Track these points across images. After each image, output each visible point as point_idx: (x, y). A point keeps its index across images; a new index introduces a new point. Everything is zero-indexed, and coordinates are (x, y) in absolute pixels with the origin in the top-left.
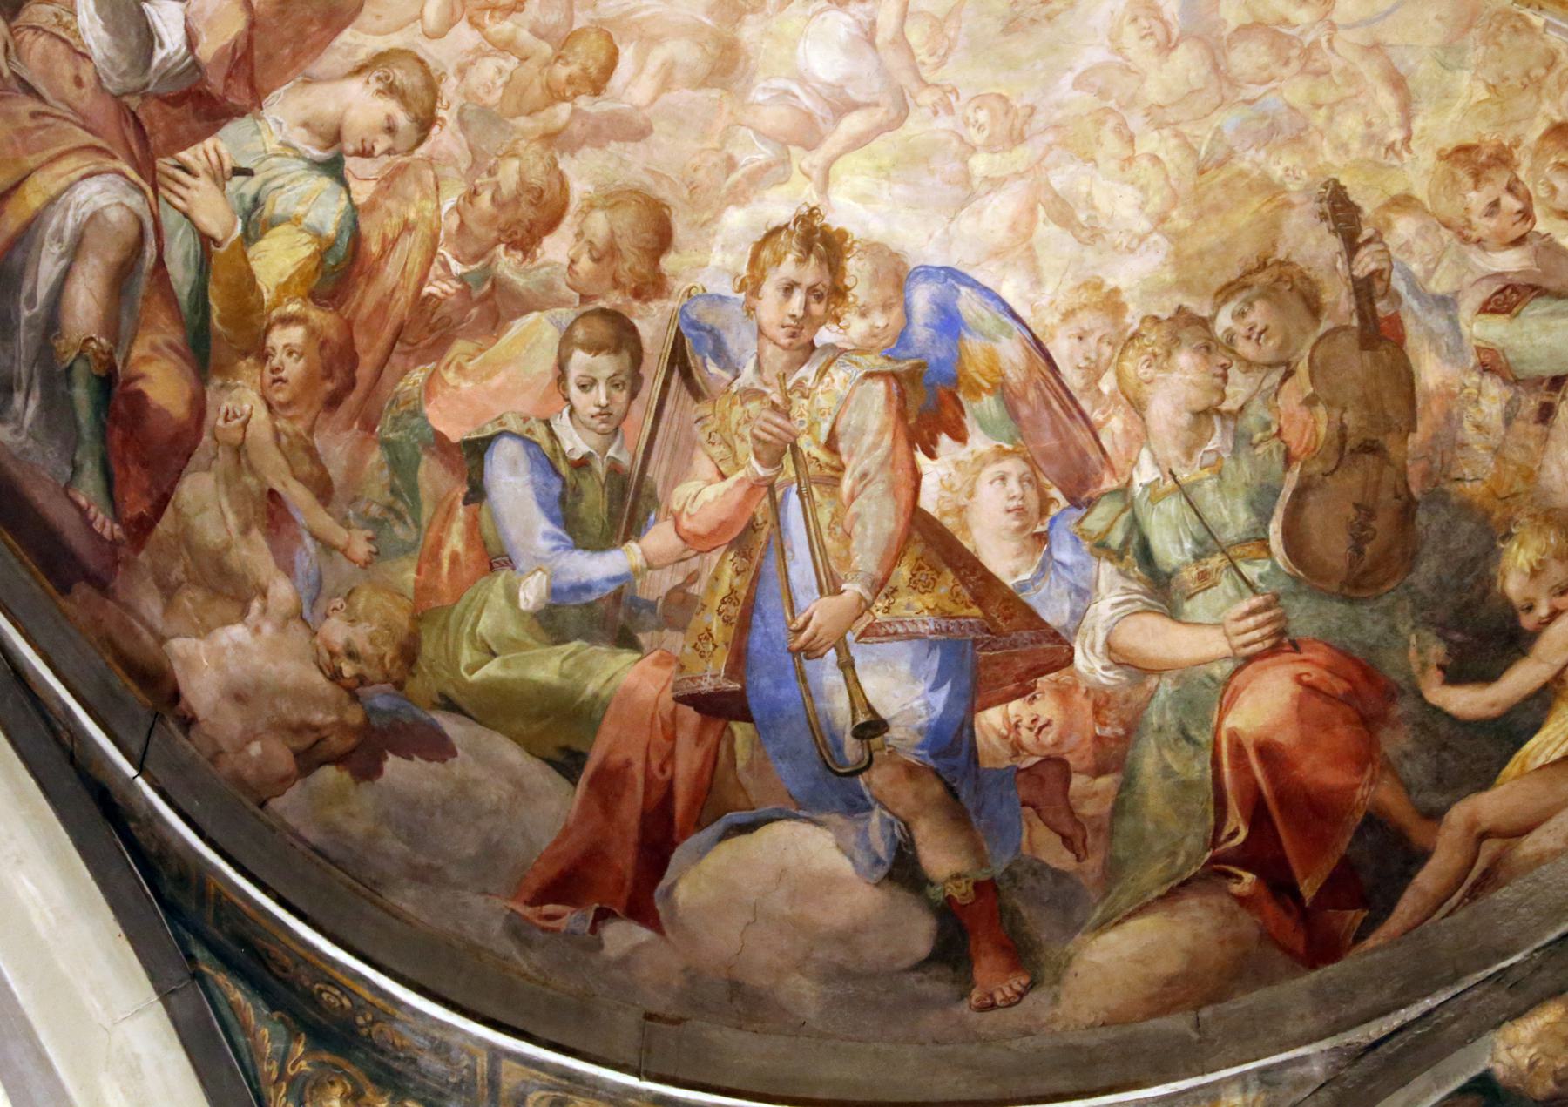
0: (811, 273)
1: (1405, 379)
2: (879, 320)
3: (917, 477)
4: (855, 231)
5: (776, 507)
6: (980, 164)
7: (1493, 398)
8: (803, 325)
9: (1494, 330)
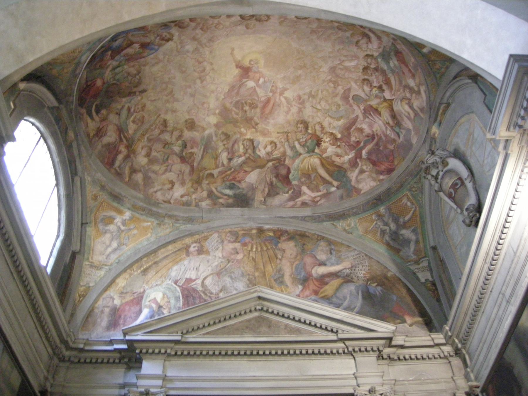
0: (166, 38)
1: (124, 97)
2: (157, 43)
3: (138, 43)
4: (168, 43)
5: (144, 31)
6: (167, 57)
7: (119, 107)
8: (161, 36)
9: (126, 107)
